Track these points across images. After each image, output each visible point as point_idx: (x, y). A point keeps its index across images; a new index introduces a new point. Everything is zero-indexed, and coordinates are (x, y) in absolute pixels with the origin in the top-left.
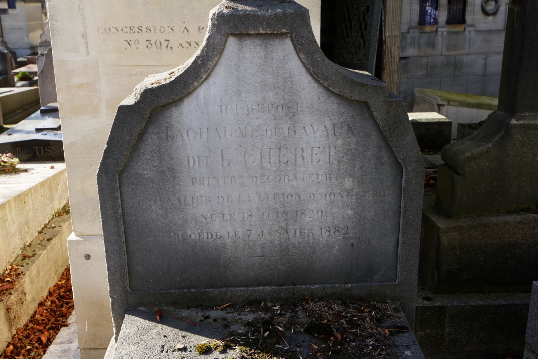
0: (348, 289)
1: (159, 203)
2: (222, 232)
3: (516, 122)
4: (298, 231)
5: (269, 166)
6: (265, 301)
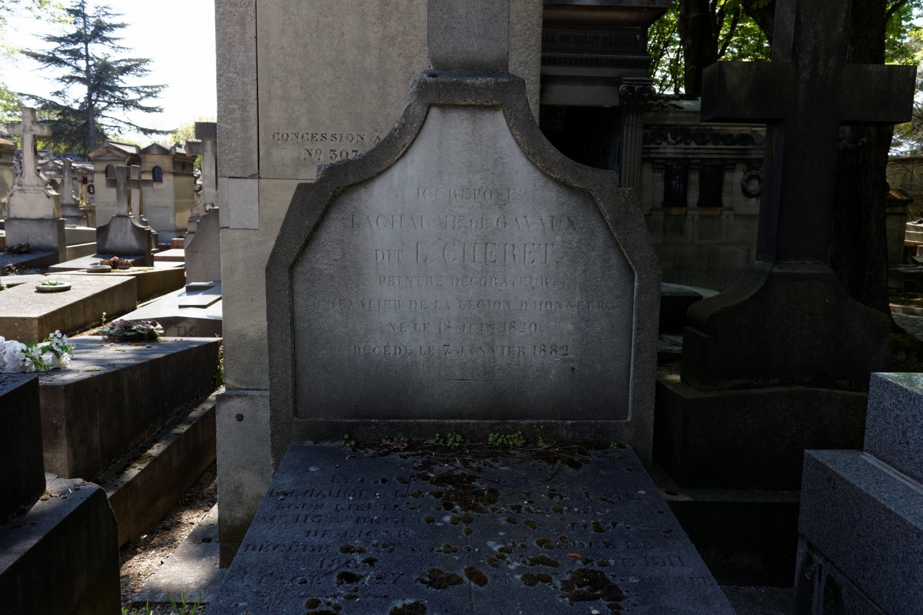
1: (337, 308)
3: (778, 270)
4: (506, 350)
5: (472, 265)
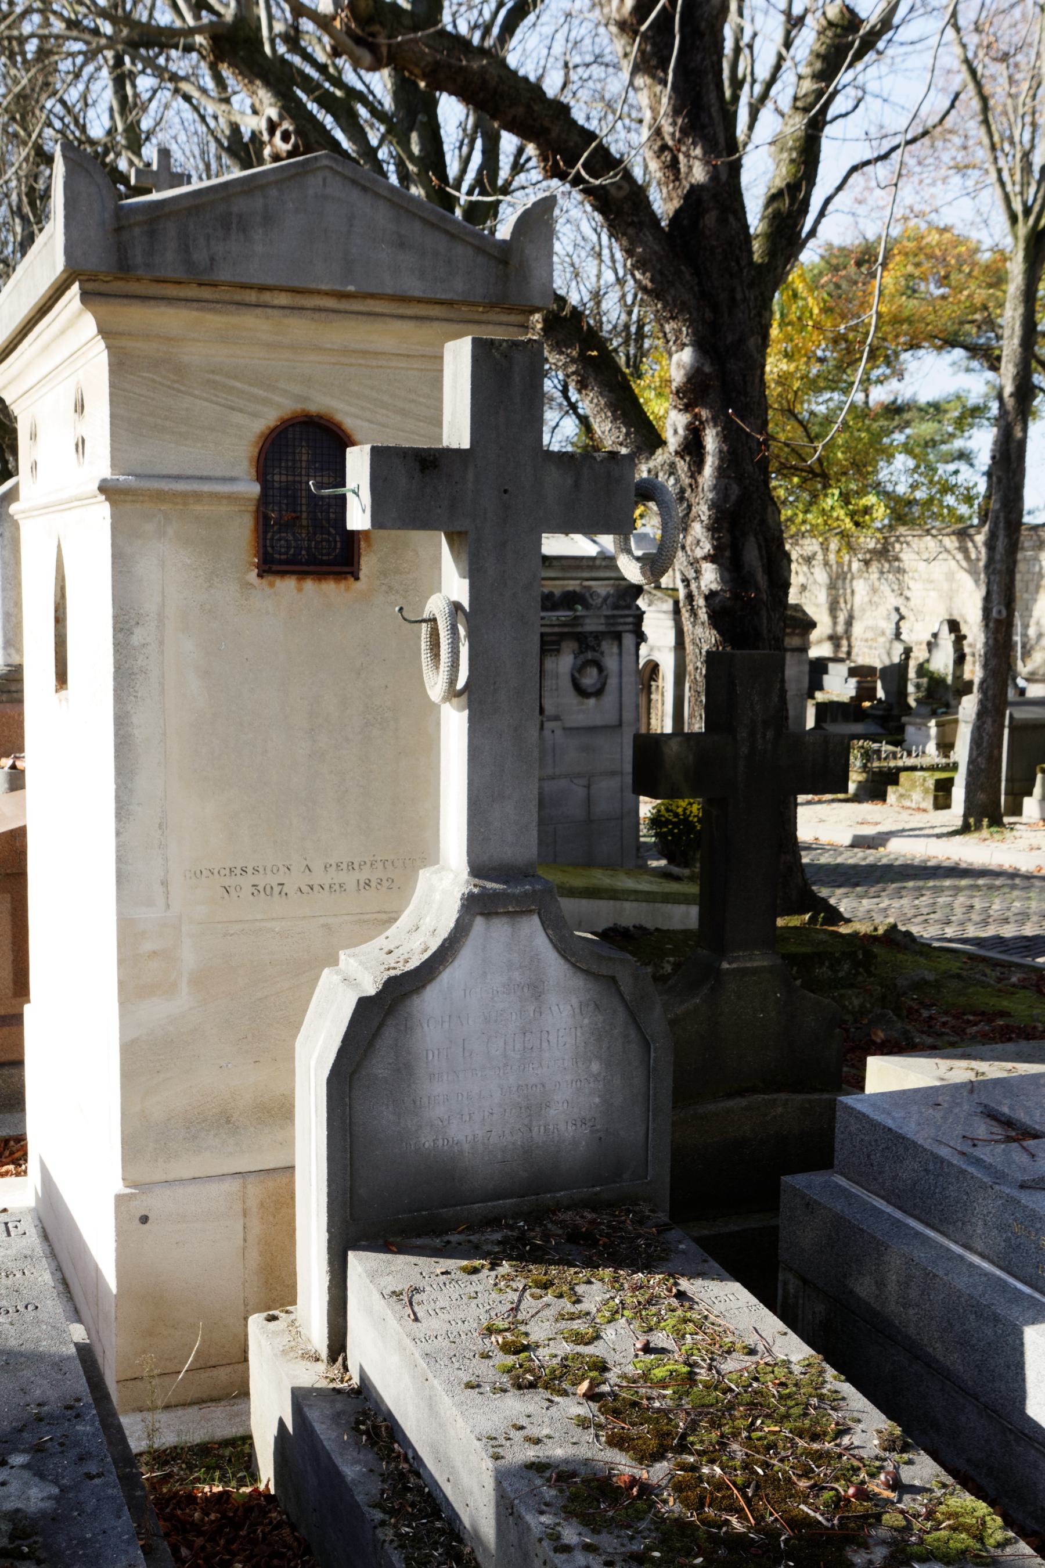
0: (596, 1194)
2: (460, 1137)
5: (512, 1054)
6: (505, 1217)
